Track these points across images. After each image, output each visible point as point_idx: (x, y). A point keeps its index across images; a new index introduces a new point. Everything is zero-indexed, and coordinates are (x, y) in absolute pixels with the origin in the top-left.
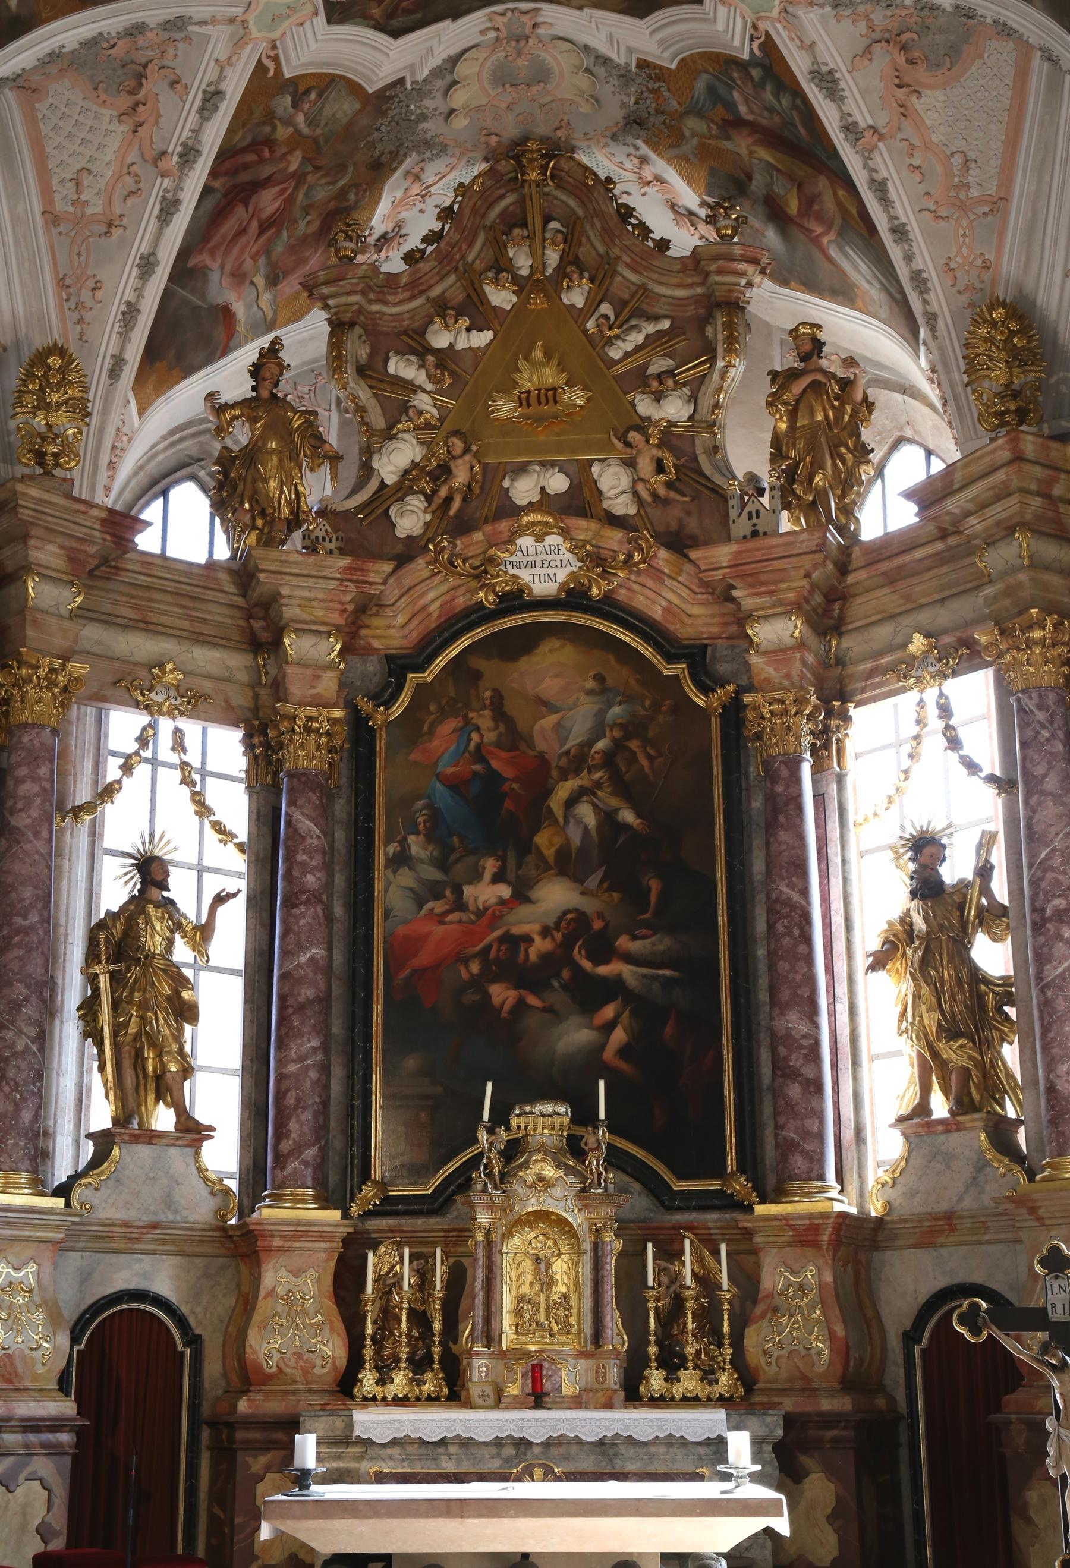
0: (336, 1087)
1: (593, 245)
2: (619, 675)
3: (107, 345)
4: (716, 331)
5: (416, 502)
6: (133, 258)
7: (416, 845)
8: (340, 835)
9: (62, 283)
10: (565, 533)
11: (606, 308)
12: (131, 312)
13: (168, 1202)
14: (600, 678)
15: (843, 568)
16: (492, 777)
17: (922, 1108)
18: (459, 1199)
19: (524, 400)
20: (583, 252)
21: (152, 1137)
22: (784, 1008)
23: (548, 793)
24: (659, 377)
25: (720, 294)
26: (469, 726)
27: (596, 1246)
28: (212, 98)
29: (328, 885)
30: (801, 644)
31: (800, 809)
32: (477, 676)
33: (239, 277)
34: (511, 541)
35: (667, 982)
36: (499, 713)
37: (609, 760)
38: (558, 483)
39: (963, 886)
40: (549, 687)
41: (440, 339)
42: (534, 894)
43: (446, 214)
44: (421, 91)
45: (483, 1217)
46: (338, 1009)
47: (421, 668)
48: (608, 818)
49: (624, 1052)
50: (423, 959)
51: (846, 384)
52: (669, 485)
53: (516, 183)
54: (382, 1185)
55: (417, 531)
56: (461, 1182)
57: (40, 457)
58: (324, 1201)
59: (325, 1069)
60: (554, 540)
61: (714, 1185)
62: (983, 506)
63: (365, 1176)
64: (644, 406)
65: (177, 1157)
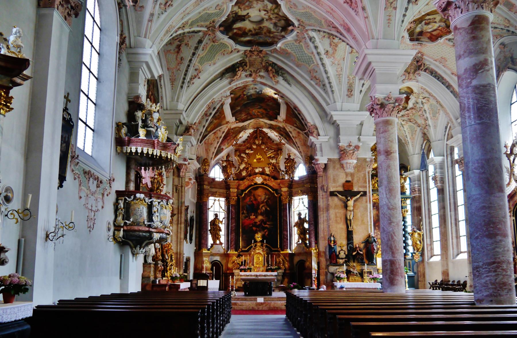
1: (265, 140)
2: (267, 192)
3: (211, 155)
4: (279, 152)
5: (245, 172)
6: (214, 147)
7: (245, 212)
10: (262, 177)
11: (267, 149)
12: (213, 153)
13: (219, 251)
16: (253, 204)
17: (299, 241)
18: (250, 251)
19: (257, 160)
20: (264, 141)
21: (217, 244)
22: (284, 231)
23: (259, 206)
24: (272, 157)
26: (251, 198)
28: (223, 132)
30: (288, 191)
32: (251, 192)
33: (224, 145)
34: (255, 178)
36: (254, 196)
37: (266, 202)
38: (261, 170)
40: (260, 194)
41: (247, 152)
43: (248, 137)
45: (252, 253)
48: (266, 209)
49: (267, 235)
50: (245, 224)
51: (293, 160)
54: (241, 249)
57: (205, 171)
58: (236, 251)
59: (235, 237)
60: (260, 178)
62: (306, 180)
63: (240, 248)
64: (271, 161)
65: (220, 246)
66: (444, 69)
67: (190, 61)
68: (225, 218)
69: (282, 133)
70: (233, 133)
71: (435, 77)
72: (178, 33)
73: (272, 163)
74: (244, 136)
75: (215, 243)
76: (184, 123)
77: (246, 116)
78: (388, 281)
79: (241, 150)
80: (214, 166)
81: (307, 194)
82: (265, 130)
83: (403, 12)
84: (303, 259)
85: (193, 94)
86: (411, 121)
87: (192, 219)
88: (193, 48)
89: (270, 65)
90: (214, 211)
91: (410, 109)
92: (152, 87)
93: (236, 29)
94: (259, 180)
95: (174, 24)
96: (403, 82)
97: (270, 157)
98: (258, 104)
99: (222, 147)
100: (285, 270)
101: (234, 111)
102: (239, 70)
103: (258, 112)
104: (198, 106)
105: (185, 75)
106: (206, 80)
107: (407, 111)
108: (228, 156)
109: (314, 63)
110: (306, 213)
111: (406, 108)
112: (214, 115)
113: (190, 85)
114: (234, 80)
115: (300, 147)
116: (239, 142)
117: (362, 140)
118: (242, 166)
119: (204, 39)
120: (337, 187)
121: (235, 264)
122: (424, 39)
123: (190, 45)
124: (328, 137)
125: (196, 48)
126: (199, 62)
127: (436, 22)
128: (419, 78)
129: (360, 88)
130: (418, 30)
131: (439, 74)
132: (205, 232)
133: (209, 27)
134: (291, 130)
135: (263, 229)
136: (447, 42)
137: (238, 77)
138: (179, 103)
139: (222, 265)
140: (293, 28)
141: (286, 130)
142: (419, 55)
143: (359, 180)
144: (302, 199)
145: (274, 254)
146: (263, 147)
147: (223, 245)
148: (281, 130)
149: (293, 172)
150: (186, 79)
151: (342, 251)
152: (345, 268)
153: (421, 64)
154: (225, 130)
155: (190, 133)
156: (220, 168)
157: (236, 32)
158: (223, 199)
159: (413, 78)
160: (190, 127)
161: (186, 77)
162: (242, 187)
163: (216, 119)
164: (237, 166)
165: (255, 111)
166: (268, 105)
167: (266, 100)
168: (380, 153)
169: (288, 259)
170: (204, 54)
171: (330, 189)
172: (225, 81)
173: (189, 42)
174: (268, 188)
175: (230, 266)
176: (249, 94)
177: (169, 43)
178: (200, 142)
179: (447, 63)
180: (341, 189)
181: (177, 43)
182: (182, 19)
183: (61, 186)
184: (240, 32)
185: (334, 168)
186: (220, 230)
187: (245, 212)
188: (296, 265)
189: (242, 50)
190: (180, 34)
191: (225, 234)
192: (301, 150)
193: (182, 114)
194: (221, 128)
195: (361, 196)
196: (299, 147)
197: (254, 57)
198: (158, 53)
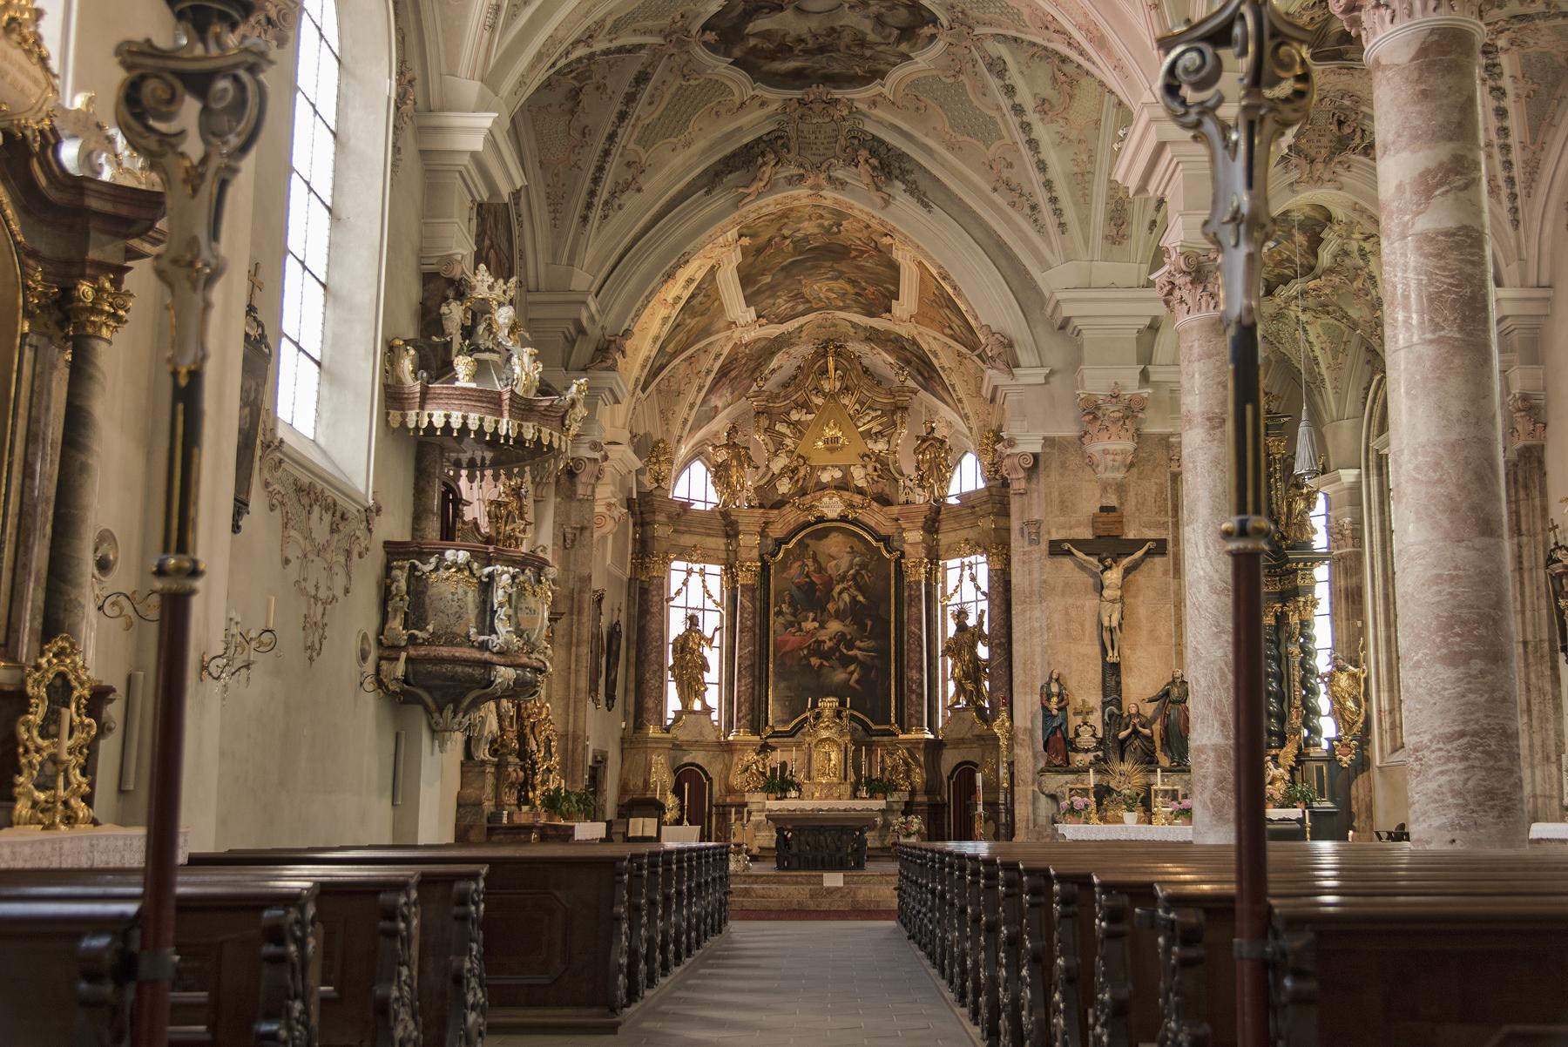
0: (756, 693)
1: (853, 380)
2: (859, 546)
3: (676, 432)
4: (898, 417)
5: (786, 480)
6: (687, 404)
7: (785, 608)
8: (758, 604)
9: (661, 412)
10: (840, 496)
11: (857, 407)
12: (685, 421)
13: (701, 734)
14: (852, 547)
15: (938, 511)
16: (812, 583)
20: (850, 383)
21: (695, 712)
25: (899, 404)
26: (804, 565)
27: (846, 748)
28: (718, 356)
29: (754, 625)
30: (923, 541)
31: (920, 600)
32: (808, 546)
33: (721, 396)
35: (873, 658)
37: (854, 577)
38: (838, 474)
39: (975, 627)
40: (834, 551)
41: (795, 416)
42: (827, 626)
43: (799, 367)
44: (789, 333)
46: (757, 665)
47: (787, 543)
48: (854, 598)
49: (857, 682)
50: (787, 648)
51: (942, 442)
52: (879, 476)
53: (825, 356)
54: (772, 727)
55: (786, 491)
56: (800, 726)
57: (657, 480)
59: (753, 688)
60: (836, 499)
61: (887, 727)
63: (767, 724)
67: (612, 137)
68: (721, 628)
69: (908, 354)
70: (750, 357)
72: (574, 56)
73: (873, 453)
74: (783, 364)
75: (686, 710)
76: (594, 332)
77: (790, 304)
78: (1208, 809)
79: (776, 411)
80: (686, 465)
81: (986, 551)
82: (854, 346)
84: (971, 758)
85: (619, 243)
86: (1328, 313)
87: (614, 632)
88: (620, 97)
89: (863, 144)
90: (686, 608)
91: (1324, 272)
92: (491, 221)
93: (755, 35)
94: (831, 507)
95: (560, 34)
97: (868, 434)
98: (827, 264)
99: (716, 401)
100: (913, 793)
101: (750, 291)
102: (765, 163)
103: (830, 290)
104: (634, 280)
105: (596, 181)
106: (660, 198)
107: (1315, 278)
108: (733, 430)
109: (1002, 137)
110: (983, 612)
112: (688, 302)
113: (611, 213)
114: (749, 194)
115: (965, 401)
116: (768, 386)
117: (1153, 378)
118: (777, 465)
119: (655, 68)
120: (1071, 528)
121: (752, 774)
123: (609, 91)
124: (1047, 371)
125: (631, 98)
126: (638, 142)
128: (1346, 178)
132: (655, 672)
133: (670, 34)
134: (935, 346)
135: (846, 661)
137: (762, 184)
138: (577, 270)
139: (710, 779)
140: (933, 31)
141: (919, 347)
143: (1143, 504)
144: (971, 568)
145: (877, 744)
146: (846, 401)
147: (714, 716)
148: (903, 348)
149: (944, 481)
150: (598, 193)
151: (1089, 730)
152: (1092, 779)
154: (722, 347)
155: (610, 362)
156: (708, 469)
157: (755, 46)
158: (716, 569)
160: (610, 341)
161: (599, 190)
162: (777, 531)
163: (693, 315)
164: (762, 463)
165: (820, 287)
166: (861, 268)
167: (854, 253)
168: (1189, 421)
169: (922, 759)
170: (656, 115)
171: (1049, 532)
172: (720, 200)
173: (608, 82)
174: (861, 532)
175: (737, 780)
176: (799, 235)
177: (548, 85)
178: (643, 390)
180: (1086, 533)
181: (570, 82)
182: (586, 15)
183: (236, 528)
184: (767, 45)
185: (1063, 466)
186: (705, 667)
187: (785, 608)
188: (949, 778)
189: (775, 101)
190: (579, 60)
191: (720, 678)
192: (968, 410)
193: (584, 303)
194: (711, 343)
195: (1148, 553)
196: (960, 401)
197: (815, 121)
198: (513, 121)
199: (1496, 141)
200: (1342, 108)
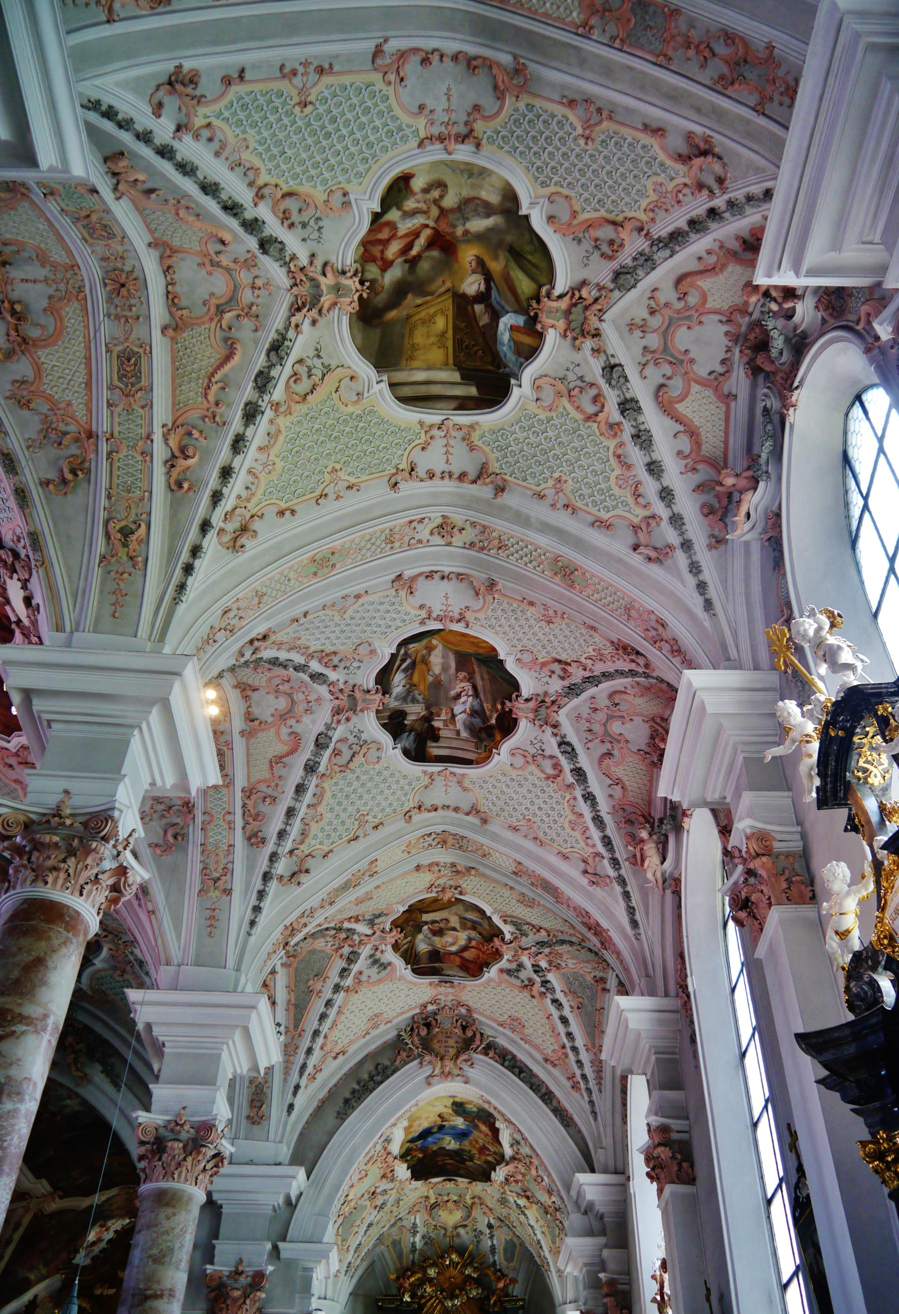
66: (526, 1046)
71: (511, 1069)
83: (253, 901)
96: (429, 1084)
111: (503, 1156)
122: (451, 969)
127: (454, 929)
128: (470, 1072)
129: (289, 1098)
130: (422, 947)
131: (522, 1062)
136: (505, 976)
142: (463, 1011)
153: (474, 1035)
159: (456, 1072)
179: (527, 1031)
199: (568, 1045)
200: (461, 1016)
